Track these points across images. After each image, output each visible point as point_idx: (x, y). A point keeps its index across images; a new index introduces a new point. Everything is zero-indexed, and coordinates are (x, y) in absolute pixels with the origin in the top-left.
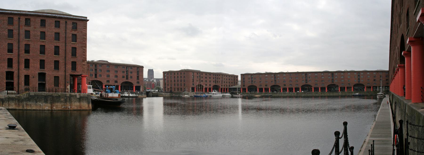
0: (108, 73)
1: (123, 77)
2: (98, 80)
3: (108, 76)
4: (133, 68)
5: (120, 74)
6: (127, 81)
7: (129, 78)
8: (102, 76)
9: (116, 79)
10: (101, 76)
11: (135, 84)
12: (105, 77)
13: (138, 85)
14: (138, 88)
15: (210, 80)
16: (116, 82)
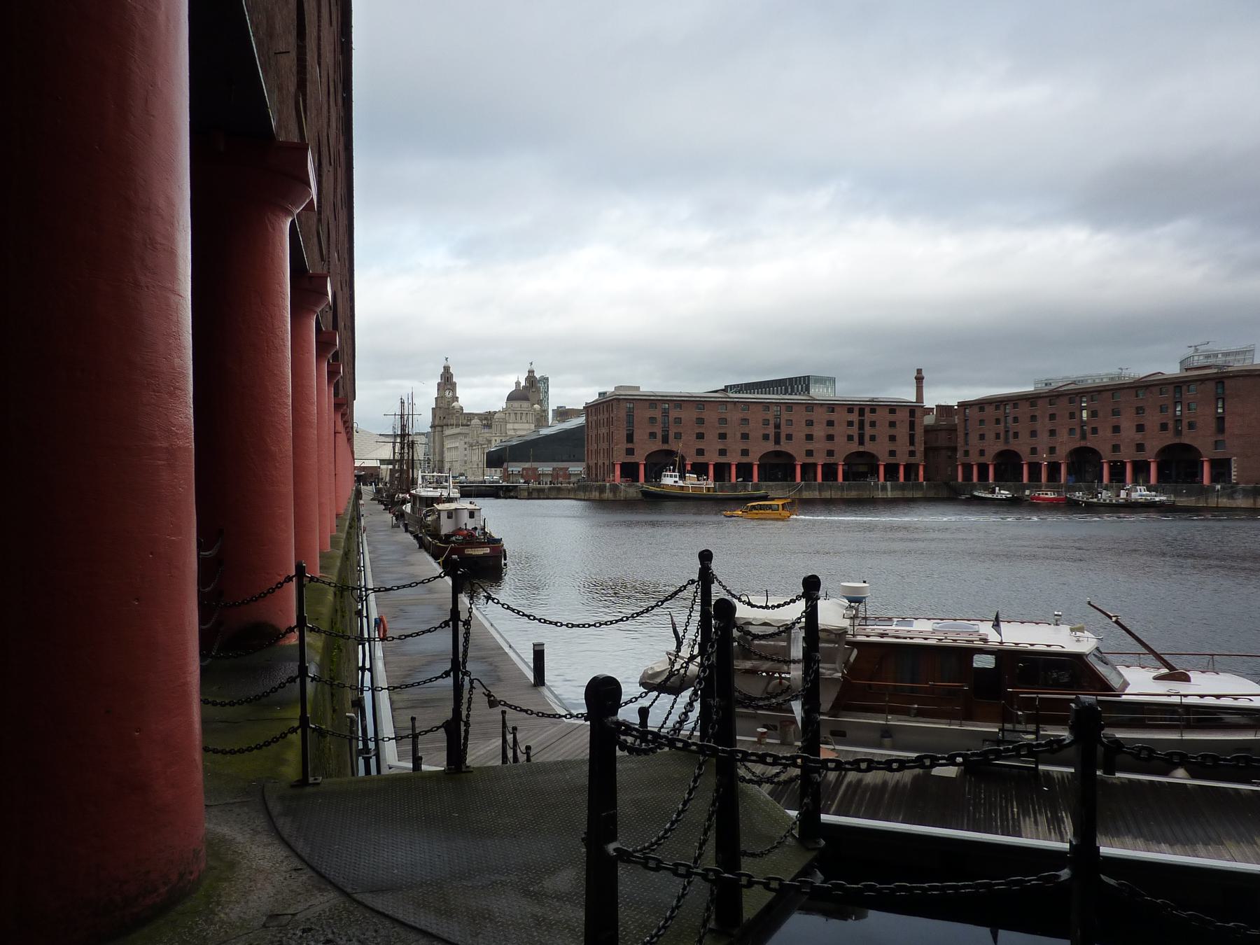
0: (1113, 420)
1: (1164, 427)
2: (1089, 445)
3: (1116, 429)
4: (987, 408)
5: (1152, 419)
6: (1177, 441)
7: (1185, 430)
8: (1100, 432)
9: (1138, 437)
10: (1095, 431)
11: (1208, 453)
12: (1109, 433)
13: (1219, 454)
14: (1221, 468)
15: (1113, 420)
16: (1140, 447)
